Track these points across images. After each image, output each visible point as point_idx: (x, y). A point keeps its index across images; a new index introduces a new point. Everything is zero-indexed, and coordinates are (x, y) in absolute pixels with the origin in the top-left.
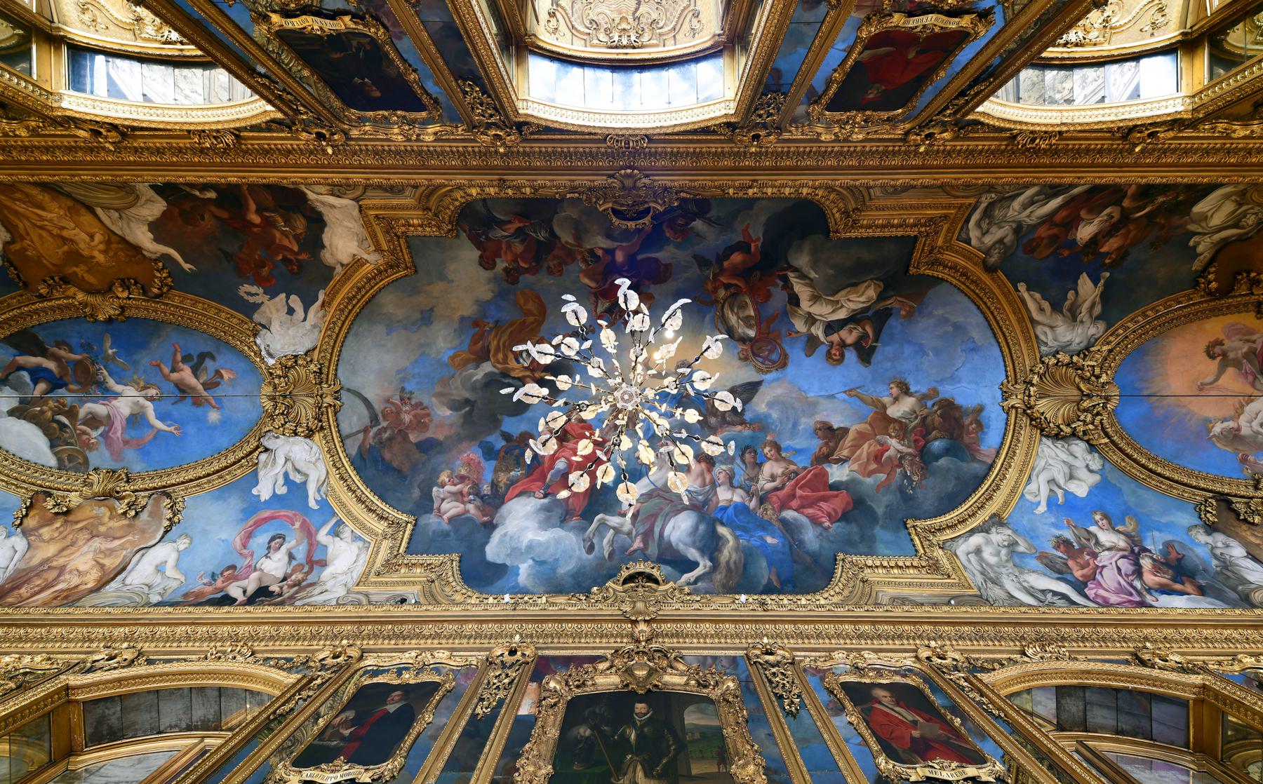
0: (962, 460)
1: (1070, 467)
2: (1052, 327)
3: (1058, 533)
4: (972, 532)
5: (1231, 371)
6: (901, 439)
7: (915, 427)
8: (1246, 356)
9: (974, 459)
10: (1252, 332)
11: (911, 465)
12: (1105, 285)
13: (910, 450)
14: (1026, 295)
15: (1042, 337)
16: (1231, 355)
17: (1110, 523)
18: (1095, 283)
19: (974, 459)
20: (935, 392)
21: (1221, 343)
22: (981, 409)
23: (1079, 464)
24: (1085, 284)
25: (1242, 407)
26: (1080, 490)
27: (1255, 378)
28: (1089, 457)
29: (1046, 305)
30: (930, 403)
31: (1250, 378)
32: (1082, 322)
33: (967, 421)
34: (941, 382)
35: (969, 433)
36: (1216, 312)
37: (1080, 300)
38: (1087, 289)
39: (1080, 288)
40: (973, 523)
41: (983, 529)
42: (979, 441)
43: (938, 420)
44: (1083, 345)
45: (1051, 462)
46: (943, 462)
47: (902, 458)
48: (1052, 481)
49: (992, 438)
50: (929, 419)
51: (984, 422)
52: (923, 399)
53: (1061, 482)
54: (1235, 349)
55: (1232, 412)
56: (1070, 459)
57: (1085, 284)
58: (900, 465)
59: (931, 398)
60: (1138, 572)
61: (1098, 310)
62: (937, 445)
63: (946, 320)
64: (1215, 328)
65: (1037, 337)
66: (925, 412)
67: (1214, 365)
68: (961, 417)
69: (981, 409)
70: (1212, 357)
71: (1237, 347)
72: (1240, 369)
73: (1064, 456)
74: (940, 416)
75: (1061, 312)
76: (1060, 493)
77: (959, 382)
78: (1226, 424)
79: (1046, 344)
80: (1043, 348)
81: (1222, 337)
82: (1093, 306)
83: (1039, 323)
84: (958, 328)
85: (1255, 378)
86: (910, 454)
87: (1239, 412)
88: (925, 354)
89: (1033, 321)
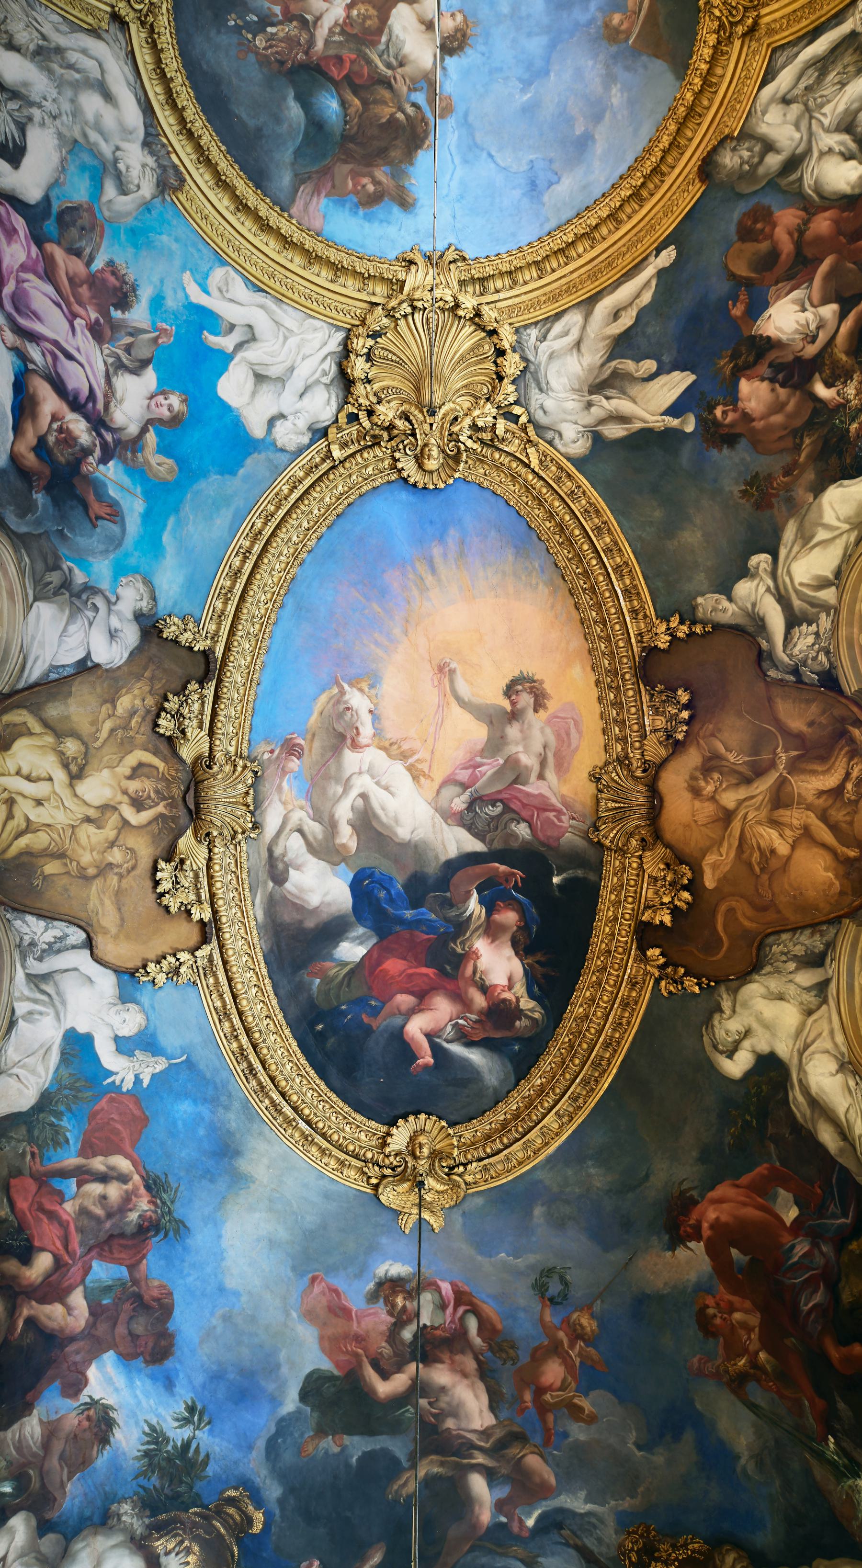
0: (298, 153)
1: (281, 381)
2: (578, 344)
3: (145, 294)
4: (147, 109)
5: (480, 733)
6: (345, 27)
7: (369, 62)
8: (512, 763)
9: (300, 180)
10: (561, 767)
11: (288, 39)
12: (669, 432)
13: (320, 44)
14: (649, 271)
15: (558, 328)
16: (513, 731)
17: (160, 421)
18: (674, 410)
19: (300, 180)
20: (447, 110)
21: (538, 706)
22: (405, 203)
23: (287, 401)
24: (675, 384)
25: (404, 756)
26: (233, 387)
27: (464, 786)
28: (302, 423)
29: (627, 320)
30: (420, 98)
31: (464, 775)
32: (589, 405)
33: (382, 173)
34: (465, 122)
35: (355, 175)
36: (607, 680)
37: (635, 390)
38: (656, 398)
39: (663, 379)
40: (166, 119)
41: (152, 139)
42: (338, 194)
43: (385, 112)
44: (539, 416)
45: (293, 341)
46: (294, 111)
47: (304, 23)
48: (251, 337)
49: (343, 225)
50: (386, 94)
51: (379, 210)
52: (428, 82)
53: (251, 354)
54: (525, 738)
55: (391, 734)
56: (296, 383)
57: (675, 384)
58: (289, 17)
59: (432, 101)
60: (59, 387)
61: (615, 431)
62: (330, 105)
63: (598, 118)
64: (574, 688)
65: (558, 316)
66: (402, 87)
67: (493, 695)
68: (390, 163)
69: (405, 203)
70: (510, 690)
71: (528, 742)
72: (482, 753)
73: (305, 371)
74: (392, 120)
75: (610, 358)
76: (227, 343)
77: (465, 161)
78: (366, 718)
79: (544, 338)
80: (534, 333)
81: (552, 705)
82: (623, 419)
83: (587, 316)
84: (583, 143)
85: (464, 786)
86: (311, 42)
87: (394, 750)
88: (527, 84)
89: (593, 300)
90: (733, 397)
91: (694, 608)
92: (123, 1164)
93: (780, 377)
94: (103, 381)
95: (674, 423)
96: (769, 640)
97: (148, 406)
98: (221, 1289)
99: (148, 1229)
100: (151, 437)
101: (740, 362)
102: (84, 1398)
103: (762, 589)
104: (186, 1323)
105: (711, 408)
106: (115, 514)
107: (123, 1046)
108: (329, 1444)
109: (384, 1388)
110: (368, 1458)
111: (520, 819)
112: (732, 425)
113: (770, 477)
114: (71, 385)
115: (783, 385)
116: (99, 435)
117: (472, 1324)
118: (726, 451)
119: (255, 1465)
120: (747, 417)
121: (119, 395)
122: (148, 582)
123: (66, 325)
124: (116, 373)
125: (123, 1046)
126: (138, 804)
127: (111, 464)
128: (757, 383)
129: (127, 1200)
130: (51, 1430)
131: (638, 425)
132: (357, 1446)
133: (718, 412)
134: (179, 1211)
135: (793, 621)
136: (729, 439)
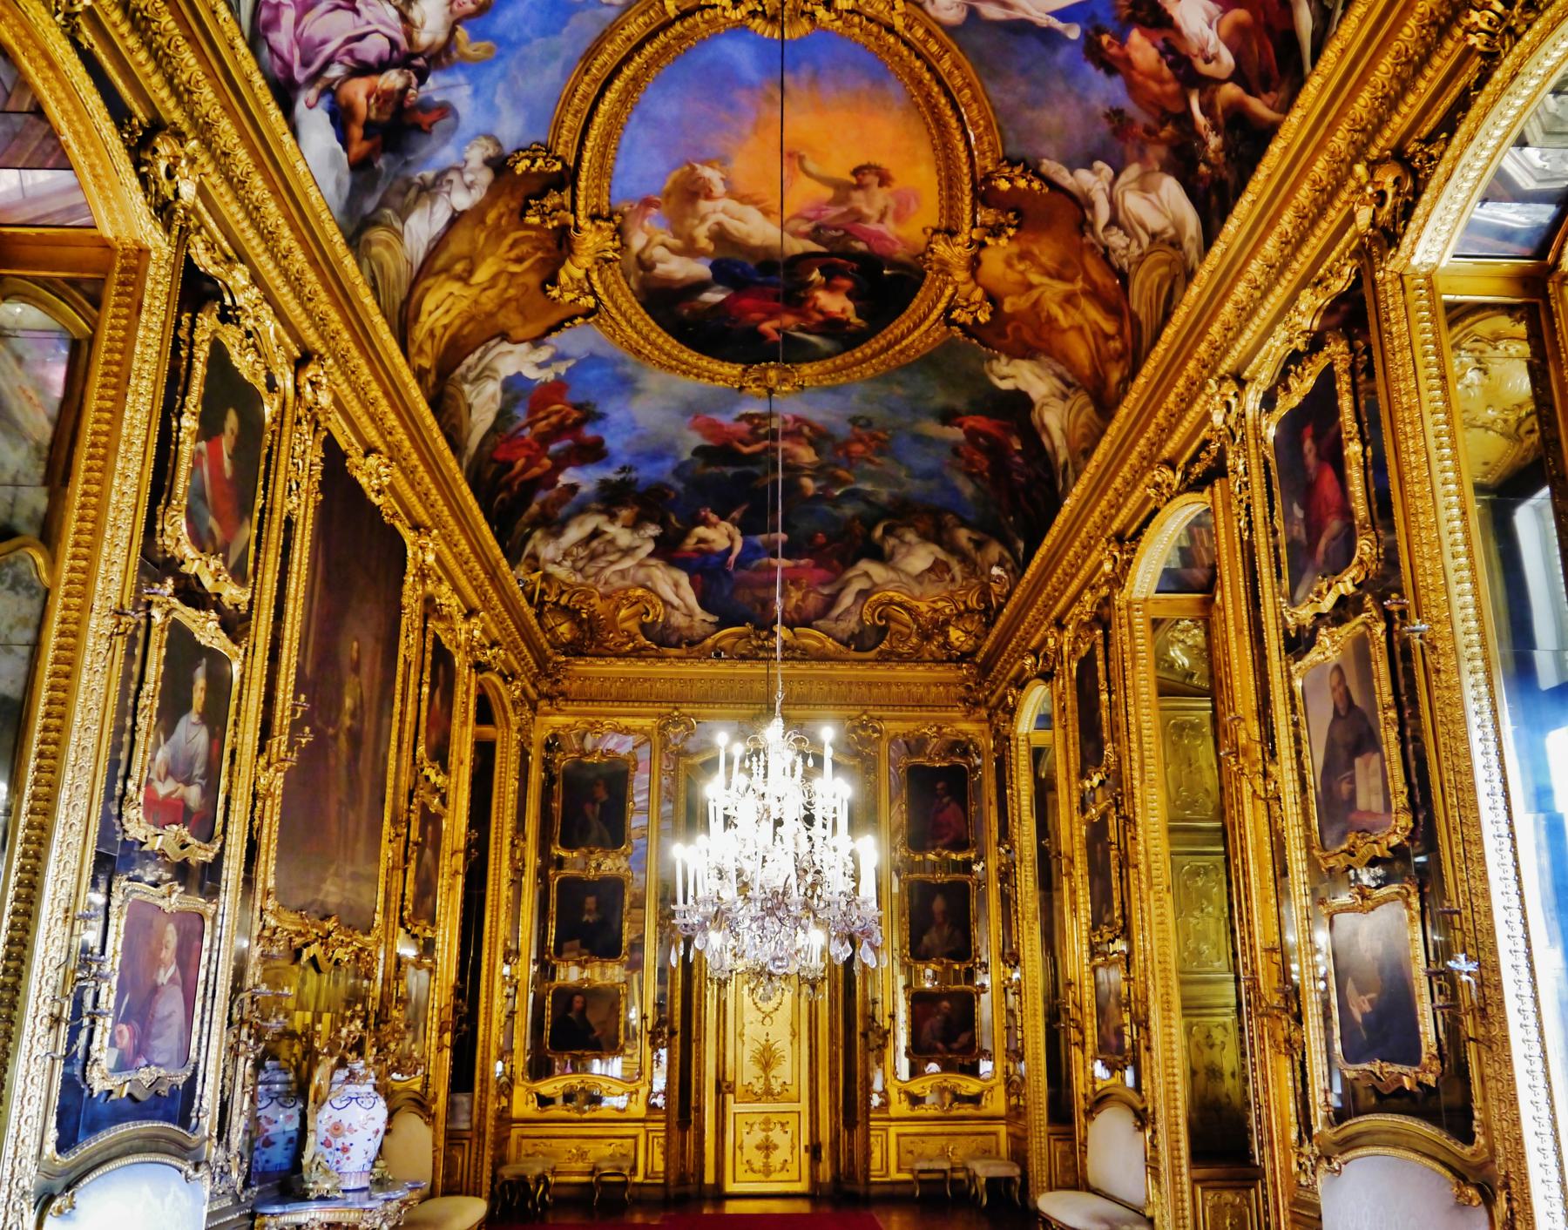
60: (363, 69)
81: (896, 186)
90: (1122, 38)
91: (1039, 165)
92: (557, 407)
93: (1170, 57)
94: (399, 25)
95: (1059, 25)
96: (1094, 215)
97: (451, 11)
98: (634, 428)
99: (579, 424)
100: (462, 33)
101: (1140, 14)
102: (559, 485)
103: (1099, 186)
104: (612, 443)
105: (1100, 31)
106: (445, 110)
107: (541, 366)
108: (712, 470)
109: (746, 450)
110: (735, 475)
111: (858, 239)
112: (1114, 57)
113: (1131, 121)
114: (371, 57)
115: (1170, 65)
116: (410, 67)
117: (806, 430)
118: (1101, 73)
119: (668, 478)
120: (1128, 61)
121: (418, 23)
122: (489, 136)
123: (350, 14)
124: (409, 7)
125: (541, 366)
126: (519, 260)
127: (429, 80)
128: (1147, 44)
129: (564, 418)
130: (543, 505)
131: (1018, 14)
132: (730, 471)
133: (1105, 39)
134: (599, 409)
135: (1114, 221)
136: (1109, 66)
